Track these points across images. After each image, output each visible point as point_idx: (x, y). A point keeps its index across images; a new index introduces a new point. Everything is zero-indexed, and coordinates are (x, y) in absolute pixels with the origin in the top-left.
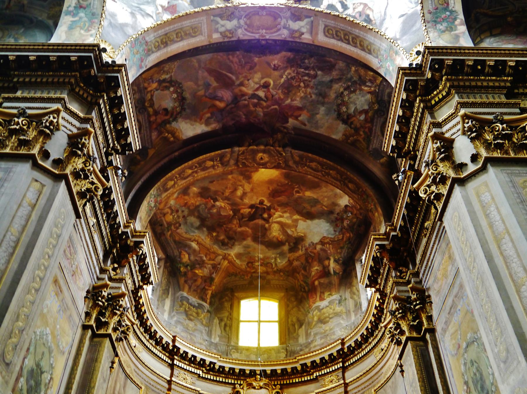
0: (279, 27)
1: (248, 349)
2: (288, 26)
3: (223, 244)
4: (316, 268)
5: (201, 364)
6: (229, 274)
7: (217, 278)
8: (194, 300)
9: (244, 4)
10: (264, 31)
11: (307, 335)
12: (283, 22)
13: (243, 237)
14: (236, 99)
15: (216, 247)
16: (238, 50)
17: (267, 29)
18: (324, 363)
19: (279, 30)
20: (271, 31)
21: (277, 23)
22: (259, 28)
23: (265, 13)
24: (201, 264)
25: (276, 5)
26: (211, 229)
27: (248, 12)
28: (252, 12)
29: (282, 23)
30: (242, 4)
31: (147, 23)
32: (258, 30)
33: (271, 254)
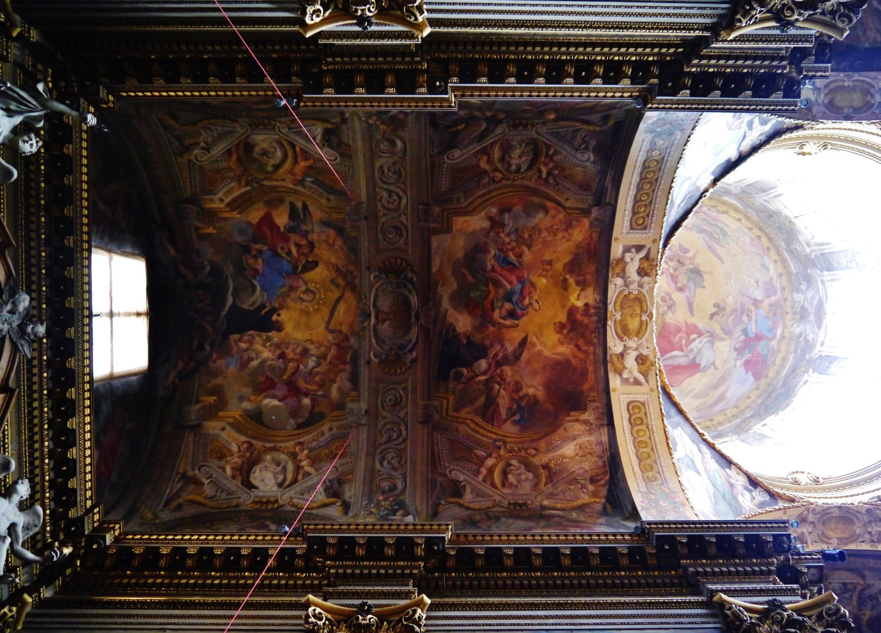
0: (826, 91)
2: (816, 92)
9: (872, 123)
10: (846, 84)
12: (822, 98)
16: (866, 49)
17: (842, 88)
19: (826, 86)
20: (836, 84)
21: (829, 96)
22: (853, 89)
23: (845, 110)
25: (830, 122)
27: (869, 113)
28: (862, 113)
29: (822, 96)
30: (875, 123)
32: (854, 86)
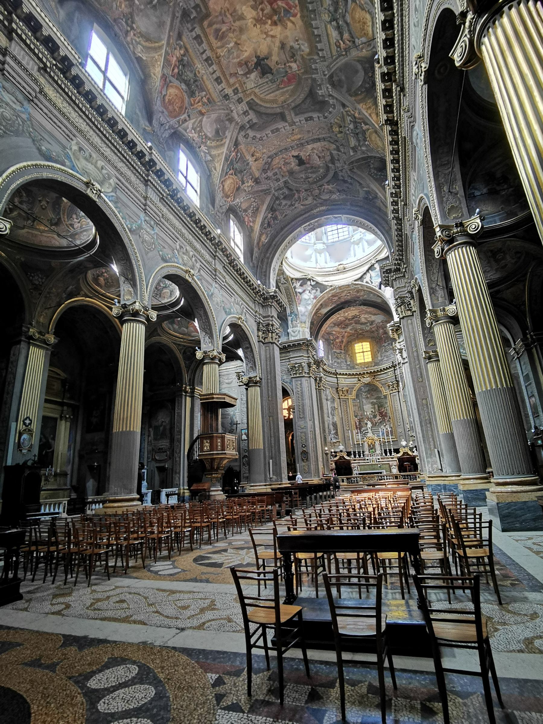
1: (360, 363)
3: (344, 328)
4: (381, 331)
5: (346, 374)
6: (348, 337)
7: (344, 340)
8: (338, 351)
11: (381, 356)
13: (351, 324)
14: (339, 298)
15: (342, 330)
18: (387, 369)
24: (338, 337)
26: (338, 326)
31: (310, 307)
33: (363, 327)
